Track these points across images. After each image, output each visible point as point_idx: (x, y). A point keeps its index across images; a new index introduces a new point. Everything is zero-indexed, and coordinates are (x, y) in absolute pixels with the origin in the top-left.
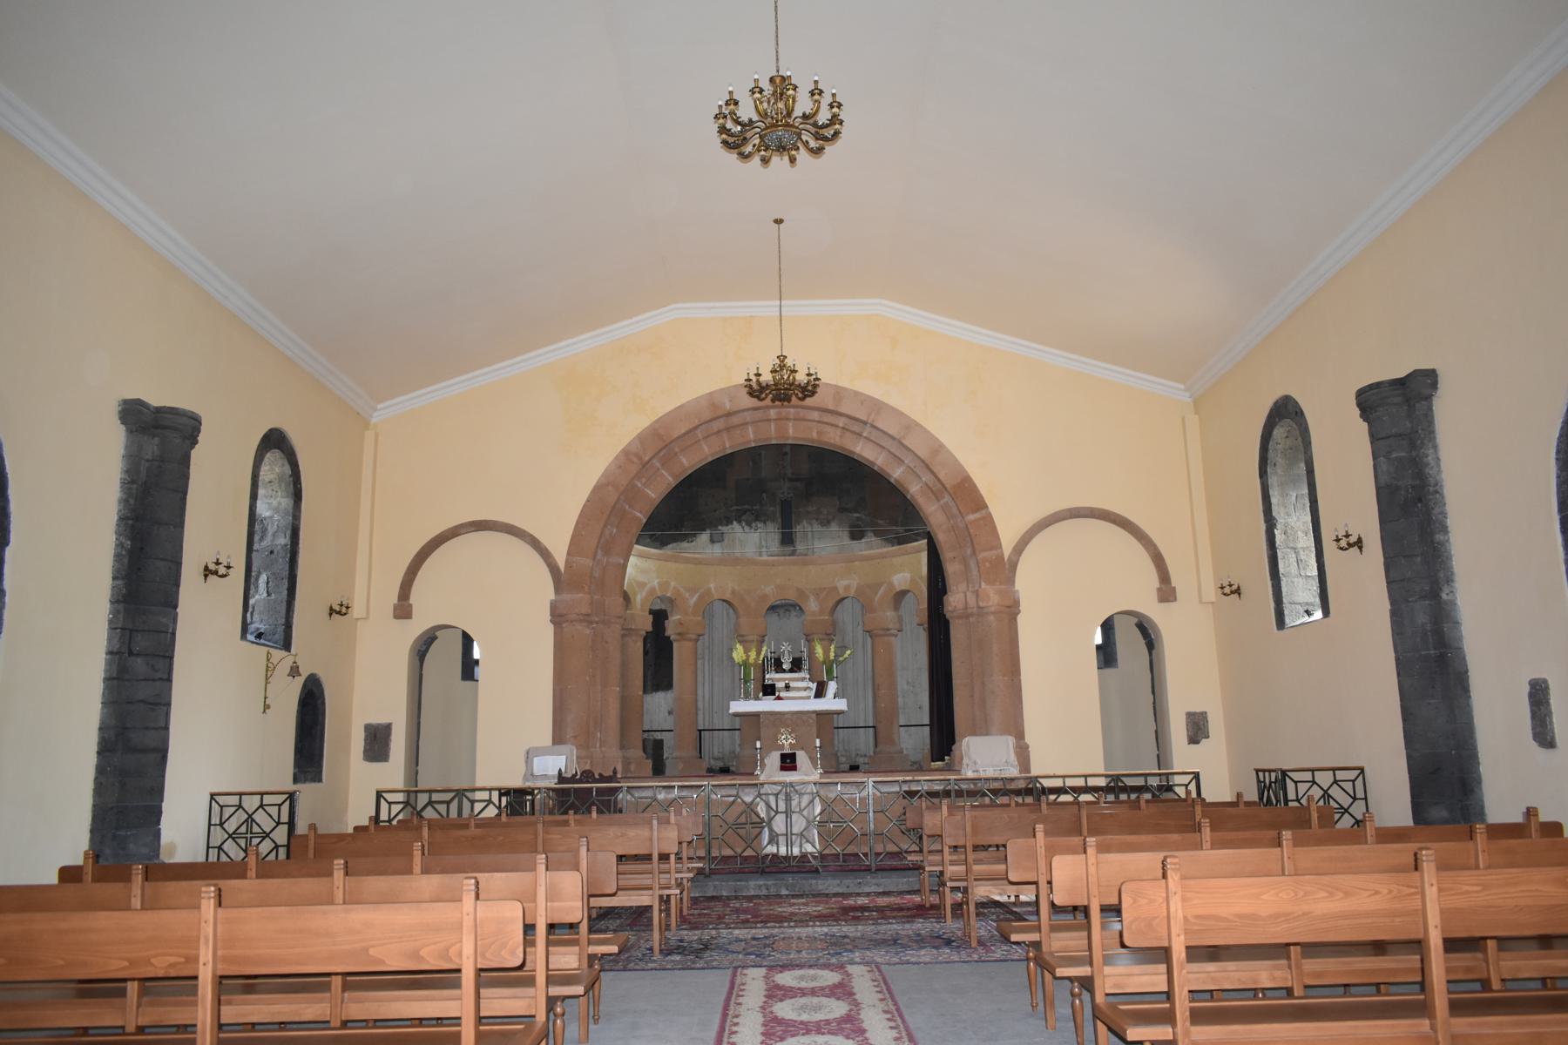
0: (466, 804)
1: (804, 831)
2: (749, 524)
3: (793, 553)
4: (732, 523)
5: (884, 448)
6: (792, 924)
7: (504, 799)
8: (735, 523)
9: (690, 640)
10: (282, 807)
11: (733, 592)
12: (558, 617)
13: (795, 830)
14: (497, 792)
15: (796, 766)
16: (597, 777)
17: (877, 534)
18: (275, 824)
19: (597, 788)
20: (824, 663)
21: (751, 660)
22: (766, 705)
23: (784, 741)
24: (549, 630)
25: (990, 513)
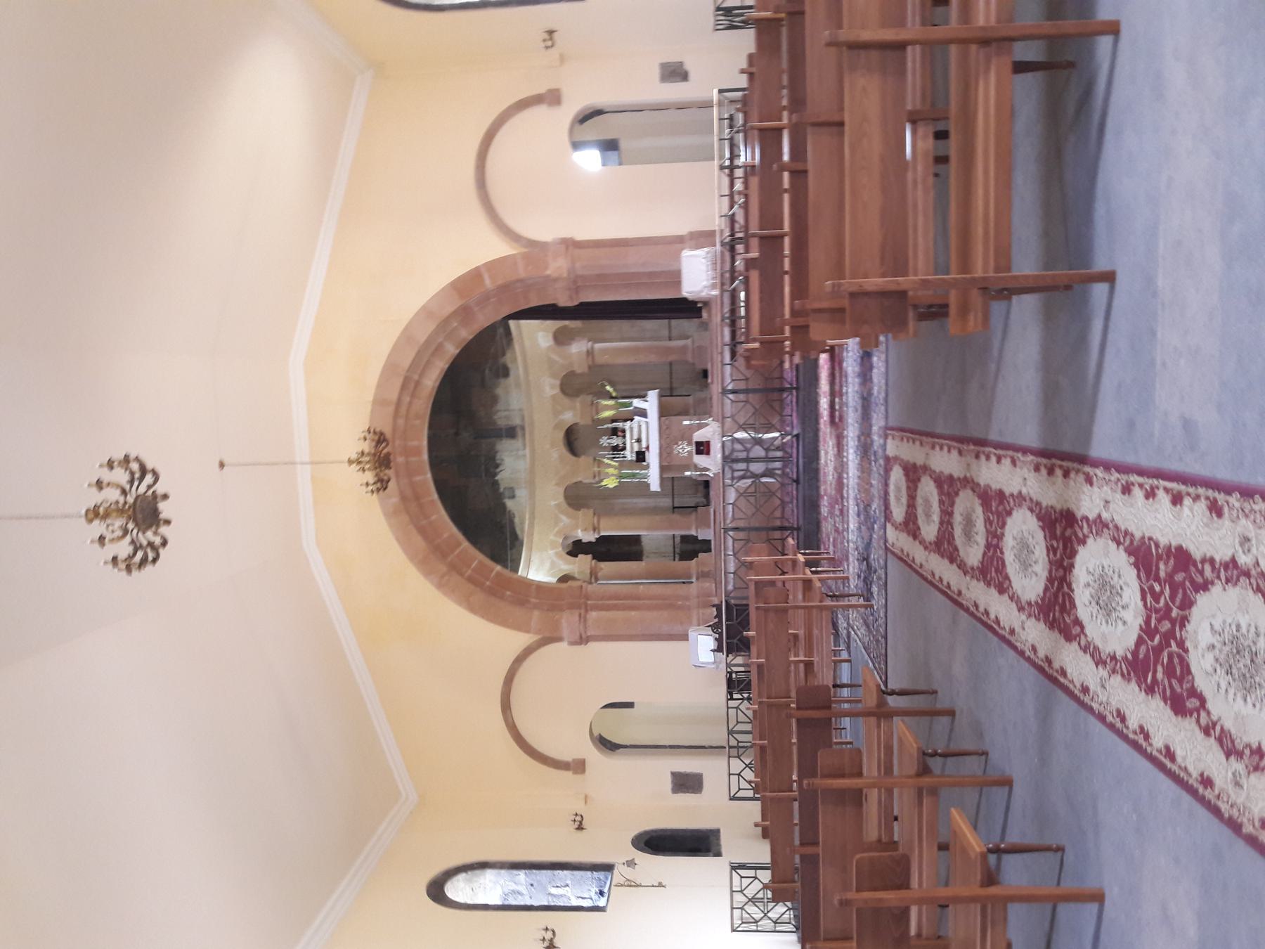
0: (740, 727)
1: (763, 448)
2: (497, 466)
3: (523, 428)
4: (497, 481)
5: (428, 362)
6: (845, 476)
7: (735, 696)
8: (496, 478)
9: (599, 522)
10: (742, 875)
11: (557, 484)
12: (583, 640)
13: (762, 453)
14: (729, 702)
15: (707, 442)
16: (716, 620)
17: (504, 354)
18: (757, 880)
19: (727, 620)
20: (617, 409)
21: (616, 472)
22: (653, 458)
23: (686, 451)
24: (593, 646)
25: (485, 265)
